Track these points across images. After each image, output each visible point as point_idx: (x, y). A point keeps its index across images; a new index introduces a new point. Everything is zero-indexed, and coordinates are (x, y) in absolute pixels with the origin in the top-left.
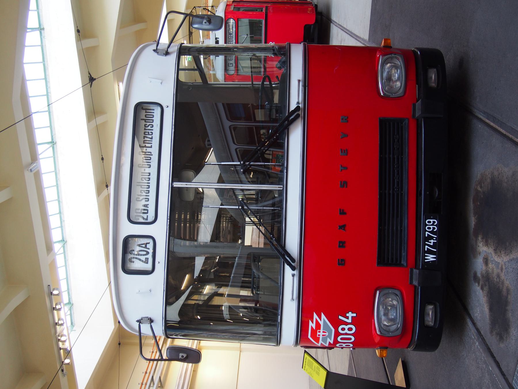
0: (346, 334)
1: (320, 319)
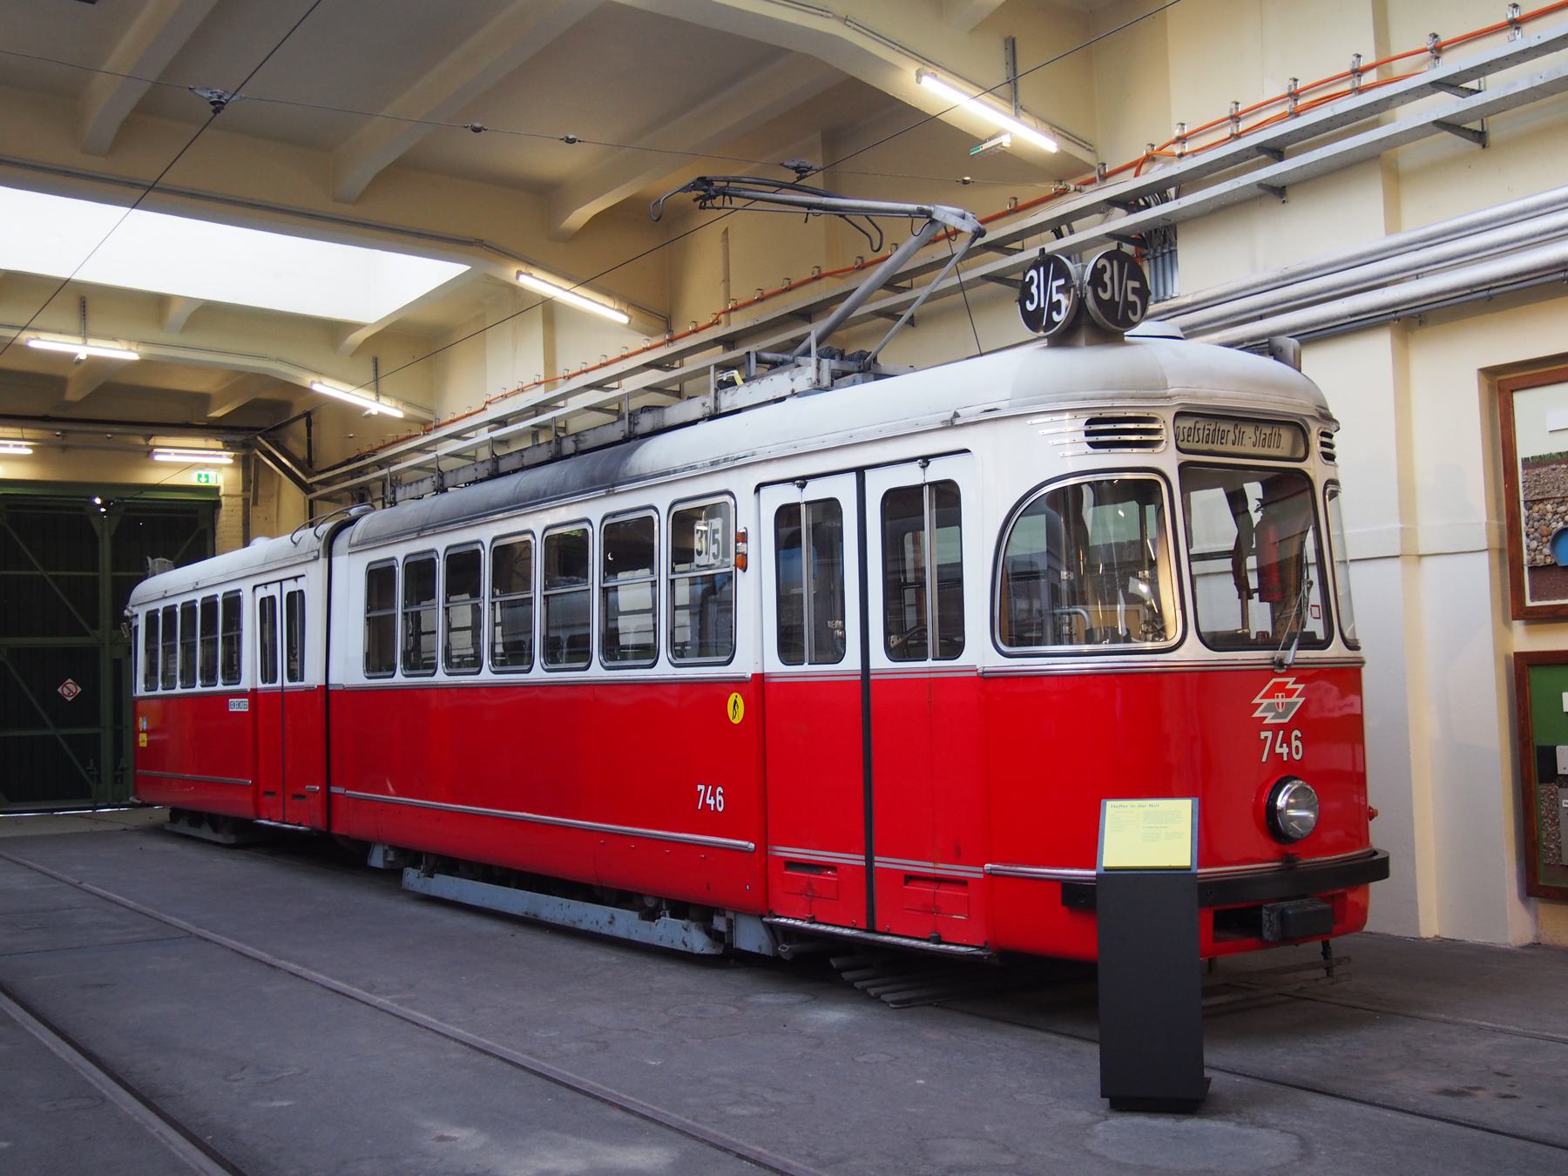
1: (1298, 696)
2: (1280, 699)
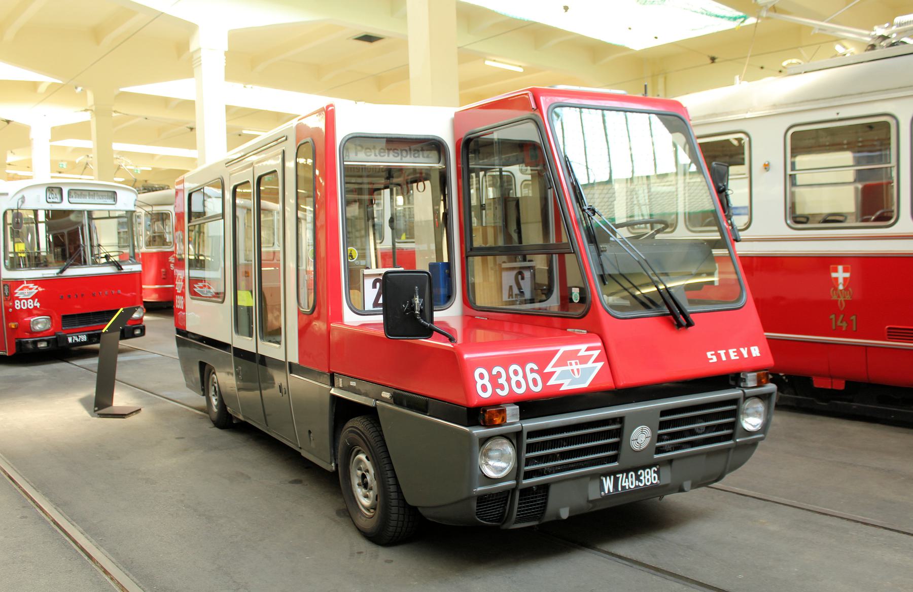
0: (27, 304)
2: (26, 291)
